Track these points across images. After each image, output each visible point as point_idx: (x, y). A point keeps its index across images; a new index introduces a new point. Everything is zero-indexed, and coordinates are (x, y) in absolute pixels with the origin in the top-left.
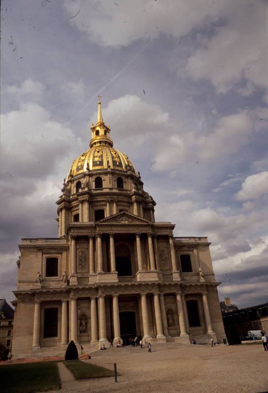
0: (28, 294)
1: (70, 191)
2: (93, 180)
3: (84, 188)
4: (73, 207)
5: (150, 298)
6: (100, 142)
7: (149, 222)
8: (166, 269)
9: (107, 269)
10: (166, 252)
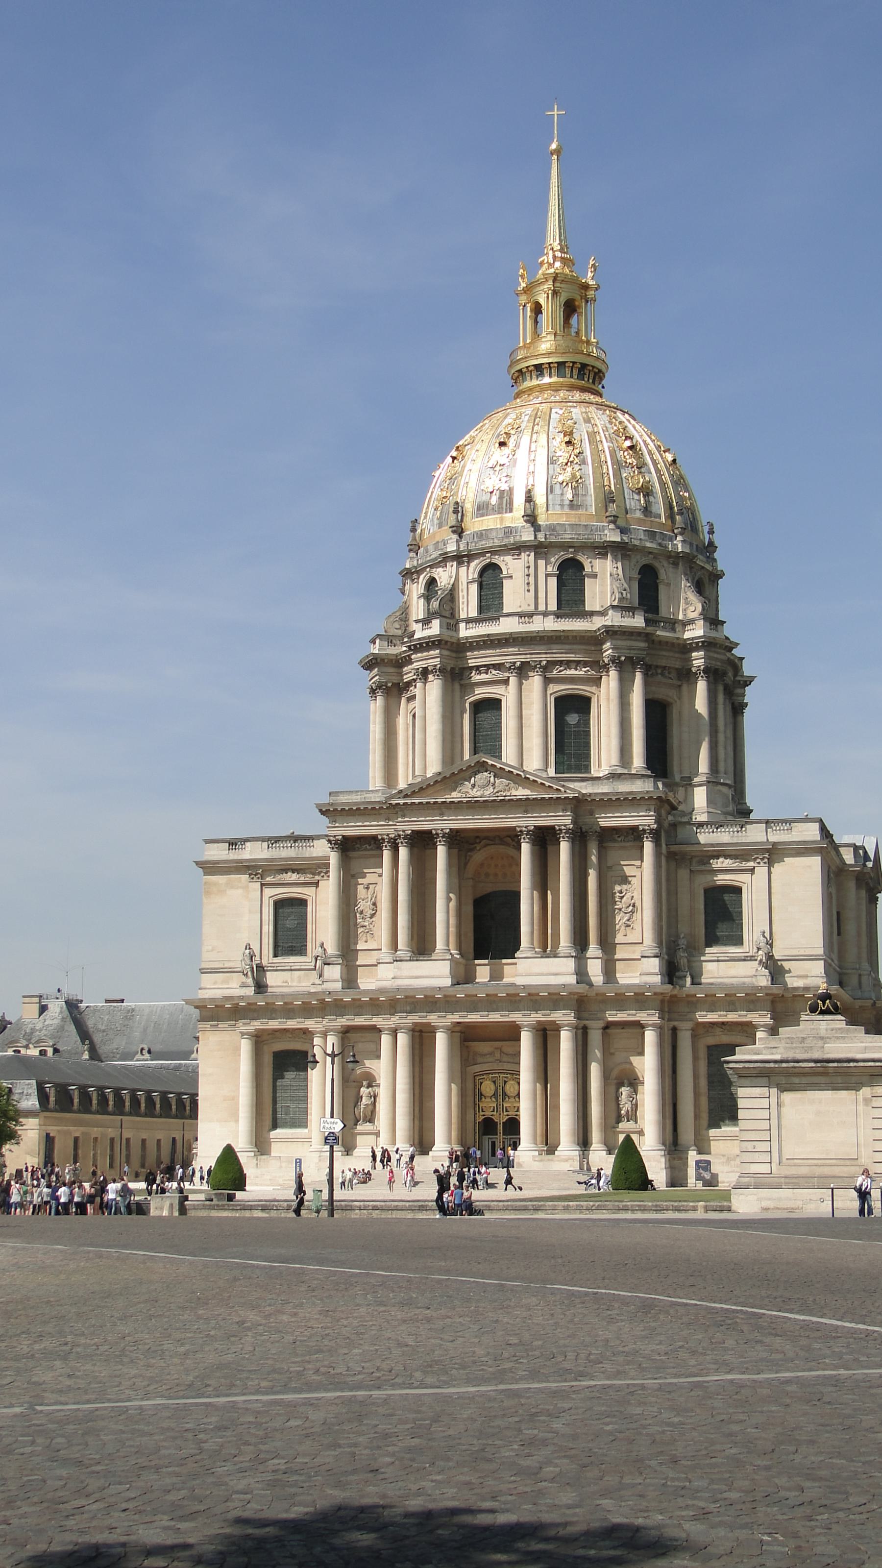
5: (546, 1036)
6: (539, 368)
7: (562, 789)
9: (422, 947)
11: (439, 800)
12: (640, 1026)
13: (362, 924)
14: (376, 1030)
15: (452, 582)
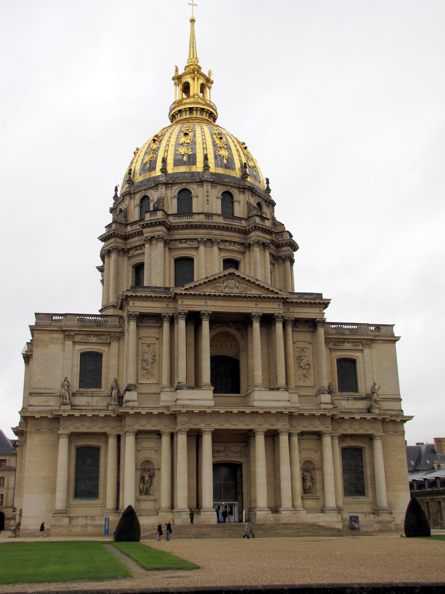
0: (47, 417)
1: (124, 213)
2: (173, 195)
3: (156, 210)
4: (132, 248)
6: (191, 109)
7: (280, 293)
8: (308, 383)
10: (309, 352)
11: (207, 294)
12: (319, 435)
13: (147, 367)
14: (159, 434)
15: (163, 196)
